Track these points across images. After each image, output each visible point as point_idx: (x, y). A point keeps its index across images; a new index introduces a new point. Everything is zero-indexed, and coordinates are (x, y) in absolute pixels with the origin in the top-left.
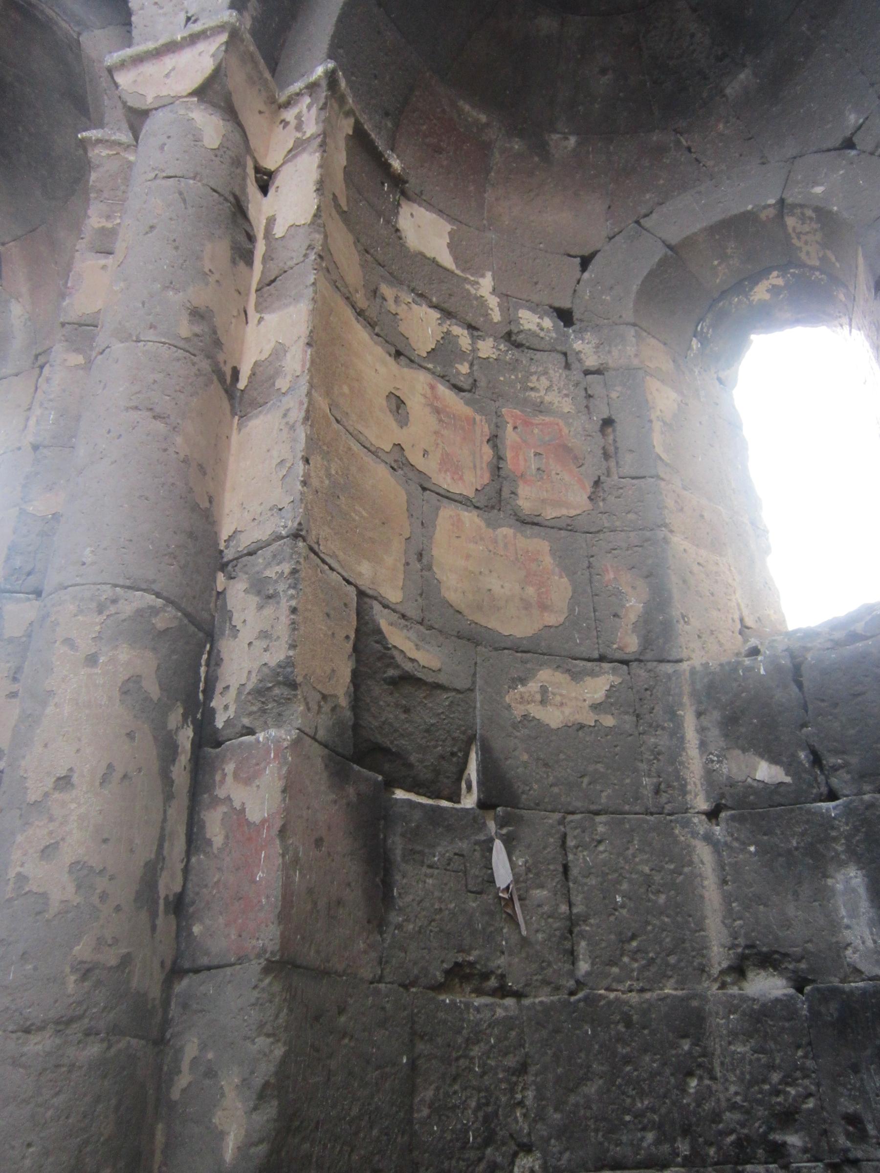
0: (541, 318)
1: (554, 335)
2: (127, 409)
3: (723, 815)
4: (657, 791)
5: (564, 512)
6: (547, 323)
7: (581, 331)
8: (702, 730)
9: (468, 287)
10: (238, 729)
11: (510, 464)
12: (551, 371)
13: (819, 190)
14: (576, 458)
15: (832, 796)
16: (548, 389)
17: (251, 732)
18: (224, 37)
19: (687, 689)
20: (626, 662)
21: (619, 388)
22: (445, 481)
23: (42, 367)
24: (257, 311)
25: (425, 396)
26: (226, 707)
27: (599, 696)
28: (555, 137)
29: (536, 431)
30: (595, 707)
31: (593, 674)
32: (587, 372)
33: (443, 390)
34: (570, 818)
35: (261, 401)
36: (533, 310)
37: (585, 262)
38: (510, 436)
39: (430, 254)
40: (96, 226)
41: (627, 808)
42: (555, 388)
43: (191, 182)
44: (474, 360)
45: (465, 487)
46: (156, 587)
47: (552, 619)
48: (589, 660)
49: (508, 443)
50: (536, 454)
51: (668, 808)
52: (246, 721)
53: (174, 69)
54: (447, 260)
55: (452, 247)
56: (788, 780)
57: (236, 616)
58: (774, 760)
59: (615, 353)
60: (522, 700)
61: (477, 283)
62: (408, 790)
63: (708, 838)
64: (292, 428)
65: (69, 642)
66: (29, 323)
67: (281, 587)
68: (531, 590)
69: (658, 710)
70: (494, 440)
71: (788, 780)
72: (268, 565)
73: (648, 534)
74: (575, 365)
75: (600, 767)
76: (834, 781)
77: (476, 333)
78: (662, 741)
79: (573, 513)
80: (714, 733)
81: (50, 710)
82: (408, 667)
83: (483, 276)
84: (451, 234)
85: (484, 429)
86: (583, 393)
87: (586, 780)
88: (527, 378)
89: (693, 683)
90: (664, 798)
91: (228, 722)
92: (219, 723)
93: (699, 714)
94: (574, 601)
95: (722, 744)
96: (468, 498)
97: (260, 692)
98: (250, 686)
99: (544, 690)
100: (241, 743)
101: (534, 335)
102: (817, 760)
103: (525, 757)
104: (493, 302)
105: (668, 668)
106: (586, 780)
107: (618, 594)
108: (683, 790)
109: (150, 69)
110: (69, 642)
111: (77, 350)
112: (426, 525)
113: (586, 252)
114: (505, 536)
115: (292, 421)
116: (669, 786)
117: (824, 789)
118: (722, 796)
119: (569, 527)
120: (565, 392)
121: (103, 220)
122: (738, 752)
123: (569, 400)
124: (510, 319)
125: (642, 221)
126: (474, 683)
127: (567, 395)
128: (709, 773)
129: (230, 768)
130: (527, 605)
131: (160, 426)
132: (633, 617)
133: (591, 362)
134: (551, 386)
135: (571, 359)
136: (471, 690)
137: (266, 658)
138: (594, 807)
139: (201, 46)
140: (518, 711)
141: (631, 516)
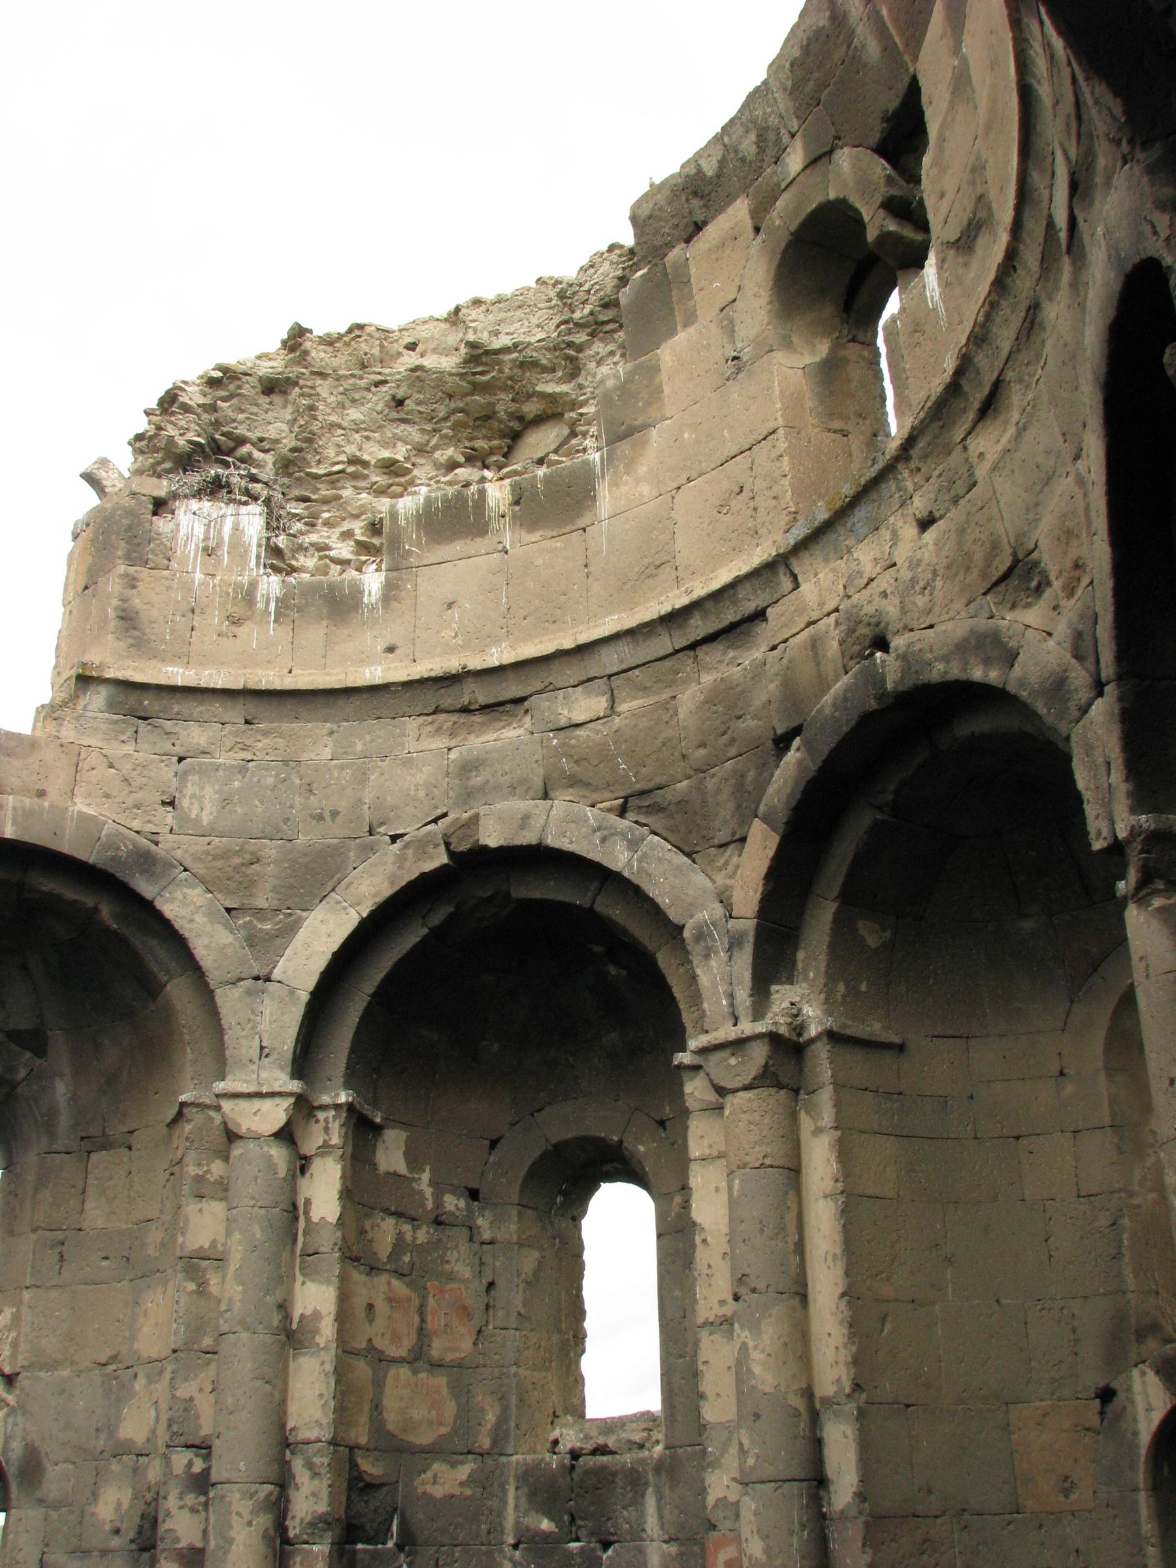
0: (458, 1199)
1: (465, 1213)
2: (253, 1379)
3: (521, 1546)
4: (489, 1532)
5: (458, 1355)
6: (462, 1203)
7: (483, 1208)
8: (517, 1498)
9: (414, 1185)
10: (301, 1540)
11: (429, 1326)
12: (460, 1246)
13: (641, 1148)
14: (469, 1314)
15: (577, 1539)
16: (458, 1260)
17: (306, 1543)
18: (292, 1100)
19: (512, 1473)
20: (481, 1455)
21: (501, 1259)
22: (393, 1352)
23: (89, 1152)
24: (302, 1274)
25: (384, 1293)
26: (294, 1528)
27: (464, 1477)
28: (484, 1043)
29: (447, 1296)
30: (462, 1484)
31: (462, 1463)
32: (482, 1243)
33: (395, 1282)
34: (442, 1548)
35: (307, 1345)
36: (454, 1194)
37: (493, 1144)
38: (431, 1302)
39: (392, 1170)
40: (193, 1173)
41: (471, 1542)
42: (461, 1259)
43: (274, 1210)
44: (416, 1248)
45: (402, 1352)
46: (271, 1480)
47: (443, 1430)
48: (461, 1454)
49: (429, 1309)
50: (445, 1314)
51: (493, 1542)
52: (305, 1537)
53: (259, 1110)
54: (402, 1168)
55: (407, 1155)
56: (557, 1530)
57: (297, 1479)
58: (551, 1519)
59: (503, 1229)
60: (423, 1483)
61: (420, 1179)
62: (363, 1543)
63: (511, 1560)
64: (327, 1375)
65: (238, 1513)
66: (71, 1103)
67: (323, 1471)
68: (434, 1413)
69: (496, 1484)
70: (421, 1310)
71: (557, 1530)
72: (315, 1455)
73: (505, 1370)
74: (476, 1238)
75: (460, 1520)
76: (580, 1534)
77: (416, 1223)
78: (494, 1503)
79: (462, 1355)
80: (523, 1500)
81: (234, 1547)
82: (368, 1479)
83: (424, 1171)
84: (406, 1142)
85: (416, 1302)
86: (478, 1262)
87: (452, 1527)
88: (444, 1254)
89: (516, 1469)
90: (492, 1536)
91: (295, 1535)
92: (291, 1534)
93: (517, 1488)
94: (458, 1416)
95: (527, 1507)
96: (404, 1358)
97: (311, 1524)
98: (306, 1521)
99: (435, 1476)
100: (303, 1549)
101: (452, 1214)
102: (573, 1520)
103: (422, 1516)
104: (428, 1192)
105: (503, 1459)
106: (452, 1527)
107: (483, 1410)
108: (502, 1532)
109: (243, 1104)
110: (238, 1513)
111: (192, 1279)
112: (379, 1384)
113: (494, 1138)
114: (422, 1379)
115: (327, 1370)
116: (495, 1530)
117: (574, 1535)
118: (522, 1536)
119: (459, 1365)
120: (467, 1261)
121: (196, 1168)
122: (534, 1512)
123: (469, 1268)
124: (439, 1204)
125: (535, 1114)
126: (399, 1477)
127: (468, 1264)
128: (517, 1523)
129: (298, 1559)
130: (431, 1423)
131: (268, 1387)
132: (489, 1426)
133: (486, 1235)
134: (459, 1258)
135: (475, 1231)
136: (397, 1481)
137: (316, 1507)
138: (455, 1542)
139: (277, 1100)
140: (420, 1491)
141: (497, 1357)
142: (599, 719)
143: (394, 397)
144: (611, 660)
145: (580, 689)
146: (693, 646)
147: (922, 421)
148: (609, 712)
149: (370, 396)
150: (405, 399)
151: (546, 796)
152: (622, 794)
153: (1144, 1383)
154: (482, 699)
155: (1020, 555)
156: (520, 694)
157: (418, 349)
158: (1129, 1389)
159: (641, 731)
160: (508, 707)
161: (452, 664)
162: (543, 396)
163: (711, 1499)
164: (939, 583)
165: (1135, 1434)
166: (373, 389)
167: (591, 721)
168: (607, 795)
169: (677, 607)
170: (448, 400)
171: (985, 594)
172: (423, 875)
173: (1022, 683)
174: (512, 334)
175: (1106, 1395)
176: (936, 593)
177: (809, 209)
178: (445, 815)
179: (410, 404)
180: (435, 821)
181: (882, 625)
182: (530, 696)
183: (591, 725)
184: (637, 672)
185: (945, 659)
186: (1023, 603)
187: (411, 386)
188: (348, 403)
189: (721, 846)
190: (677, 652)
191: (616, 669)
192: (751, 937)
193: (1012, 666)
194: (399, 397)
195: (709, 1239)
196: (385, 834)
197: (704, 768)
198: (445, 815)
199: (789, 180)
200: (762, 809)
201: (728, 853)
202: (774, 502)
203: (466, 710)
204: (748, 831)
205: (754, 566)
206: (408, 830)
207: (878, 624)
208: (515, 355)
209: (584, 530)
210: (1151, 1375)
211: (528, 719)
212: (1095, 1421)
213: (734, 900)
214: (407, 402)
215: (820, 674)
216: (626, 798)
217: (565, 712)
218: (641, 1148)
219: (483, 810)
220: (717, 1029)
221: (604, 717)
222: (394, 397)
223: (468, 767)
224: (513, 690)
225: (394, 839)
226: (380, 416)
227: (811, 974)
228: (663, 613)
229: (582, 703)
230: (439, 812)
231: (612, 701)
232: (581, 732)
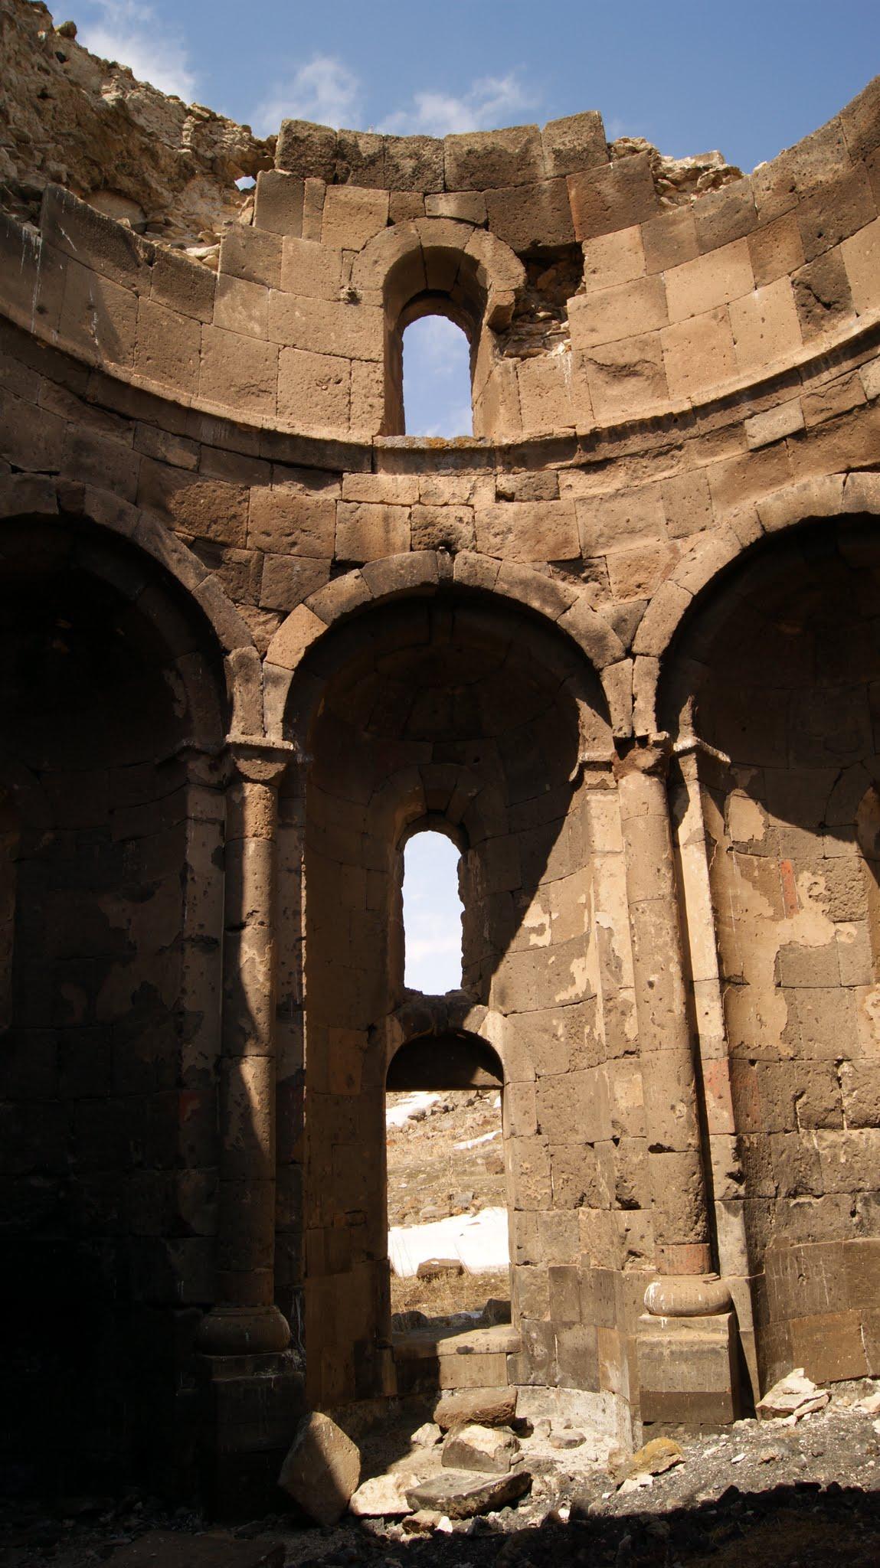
142: (187, 469)
143: (46, 88)
144: (207, 433)
145: (178, 439)
146: (272, 462)
147: (536, 442)
148: (196, 469)
149: (30, 72)
150: (51, 98)
151: (135, 504)
152: (194, 533)
153: (391, 1026)
154: (100, 399)
155: (585, 556)
156: (131, 414)
157: (65, 64)
158: (384, 1027)
159: (218, 496)
160: (116, 417)
161: (90, 357)
162: (145, 184)
163: (185, 1066)
164: (511, 537)
165: (385, 1054)
166: (36, 69)
167: (181, 468)
168: (187, 531)
169: (279, 429)
170: (74, 125)
171: (549, 562)
172: (36, 513)
173: (571, 624)
174: (149, 122)
175: (371, 1029)
176: (507, 541)
177: (444, 245)
178: (56, 474)
179: (49, 105)
180: (51, 473)
181: (453, 536)
182: (138, 420)
183: (181, 471)
184: (224, 454)
185: (511, 584)
186: (572, 580)
187: (62, 93)
188: (13, 62)
189: (263, 609)
190: (260, 458)
191: (209, 441)
192: (288, 682)
193: (564, 612)
194: (48, 92)
195: (196, 878)
196: (8, 462)
197: (266, 550)
198: (56, 474)
199: (435, 214)
200: (311, 600)
201: (270, 615)
202: (369, 408)
203: (82, 398)
204: (293, 609)
205: (351, 441)
206: (26, 469)
207: (449, 534)
208: (146, 140)
209: (201, 324)
210: (396, 1021)
211: (130, 436)
212: (365, 1045)
213: (270, 649)
214: (51, 101)
215: (387, 540)
216: (196, 538)
217: (163, 449)
218: (16, 787)
219: (89, 487)
220: (252, 734)
221: (192, 471)
222: (46, 88)
223: (81, 446)
224: (127, 408)
225: (15, 470)
226: (27, 93)
227: (295, 720)
228: (266, 427)
229: (178, 451)
230: (53, 468)
231: (199, 461)
232: (171, 471)
